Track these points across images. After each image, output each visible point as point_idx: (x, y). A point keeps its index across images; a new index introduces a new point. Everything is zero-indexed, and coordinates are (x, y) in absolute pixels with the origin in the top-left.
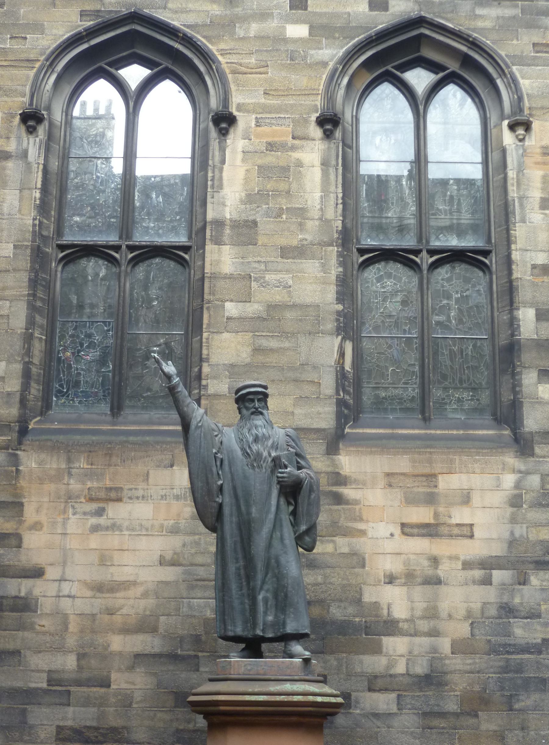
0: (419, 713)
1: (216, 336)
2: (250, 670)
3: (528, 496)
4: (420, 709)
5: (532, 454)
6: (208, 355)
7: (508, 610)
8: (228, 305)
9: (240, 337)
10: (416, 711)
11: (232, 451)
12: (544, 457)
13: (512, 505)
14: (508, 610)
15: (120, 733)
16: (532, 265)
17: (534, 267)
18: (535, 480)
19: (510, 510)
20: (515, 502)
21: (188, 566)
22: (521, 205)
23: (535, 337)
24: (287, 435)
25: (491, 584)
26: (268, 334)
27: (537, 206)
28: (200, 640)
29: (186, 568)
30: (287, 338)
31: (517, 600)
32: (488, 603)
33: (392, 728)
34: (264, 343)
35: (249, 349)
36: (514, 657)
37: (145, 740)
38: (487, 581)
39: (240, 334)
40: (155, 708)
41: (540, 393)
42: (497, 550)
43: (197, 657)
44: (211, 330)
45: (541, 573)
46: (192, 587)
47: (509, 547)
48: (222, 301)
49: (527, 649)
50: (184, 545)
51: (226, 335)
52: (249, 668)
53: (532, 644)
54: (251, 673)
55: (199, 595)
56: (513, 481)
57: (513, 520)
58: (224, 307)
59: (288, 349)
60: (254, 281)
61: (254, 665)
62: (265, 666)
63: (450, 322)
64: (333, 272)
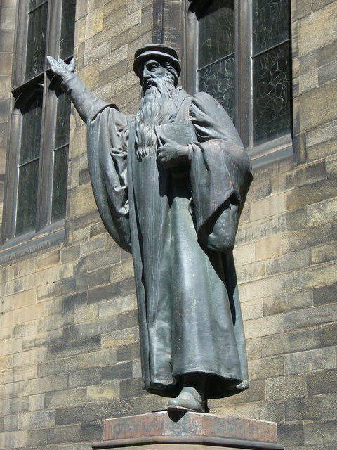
1: (304, 22)
2: (118, 433)
6: (297, 47)
21: (290, 311)
24: (193, 102)
28: (304, 404)
29: (287, 314)
39: (326, 8)
43: (300, 426)
44: (299, 17)
46: (293, 338)
50: (284, 286)
51: (313, 15)
52: (118, 430)
54: (120, 437)
55: (301, 346)
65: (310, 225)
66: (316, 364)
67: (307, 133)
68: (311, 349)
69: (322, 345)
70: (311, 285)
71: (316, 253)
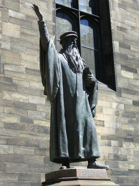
1: (5, 23)
2: (85, 175)
3: (121, 112)
5: (121, 96)
7: (117, 157)
8: (10, 11)
9: (15, 26)
11: (64, 62)
12: (125, 98)
13: (116, 115)
14: (117, 157)
16: (117, 26)
17: (118, 27)
18: (122, 106)
19: (116, 117)
20: (117, 114)
22: (113, 4)
23: (119, 52)
25: (111, 146)
26: (26, 27)
27: (117, 6)
30: (34, 31)
31: (119, 153)
32: (110, 154)
34: (25, 31)
35: (19, 32)
36: (120, 176)
38: (109, 145)
41: (122, 73)
42: (112, 132)
44: (2, 20)
45: (126, 143)
47: (116, 132)
48: (7, 8)
49: (124, 173)
51: (9, 24)
52: (84, 173)
53: (125, 171)
56: (116, 105)
57: (117, 121)
58: (8, 12)
59: (35, 36)
60: (21, 4)
61: (87, 172)
62: (91, 172)
63: (86, 42)
64: (51, 9)
65: (4, 98)
66: (4, 150)
67: (5, 64)
68: (3, 144)
69: (7, 144)
70: (3, 120)
71: (6, 110)
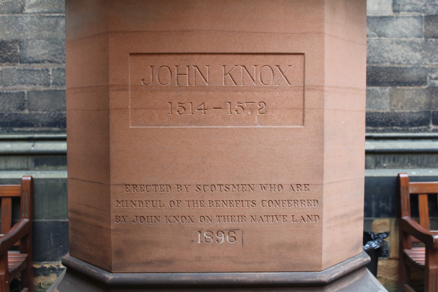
0: (421, 16)
4: (424, 11)
10: (417, 14)
15: (10, 49)
33: (384, 36)
37: (45, 57)
40: (55, 12)
